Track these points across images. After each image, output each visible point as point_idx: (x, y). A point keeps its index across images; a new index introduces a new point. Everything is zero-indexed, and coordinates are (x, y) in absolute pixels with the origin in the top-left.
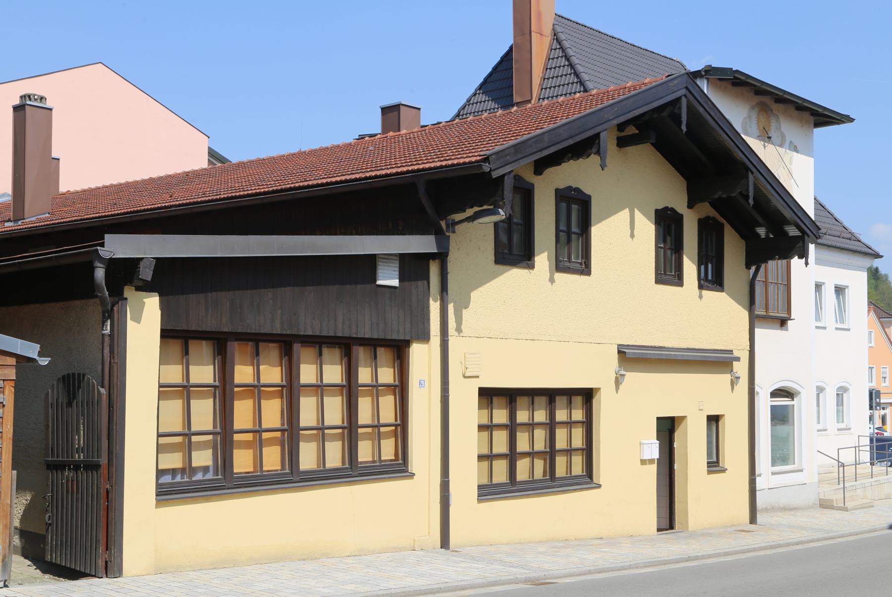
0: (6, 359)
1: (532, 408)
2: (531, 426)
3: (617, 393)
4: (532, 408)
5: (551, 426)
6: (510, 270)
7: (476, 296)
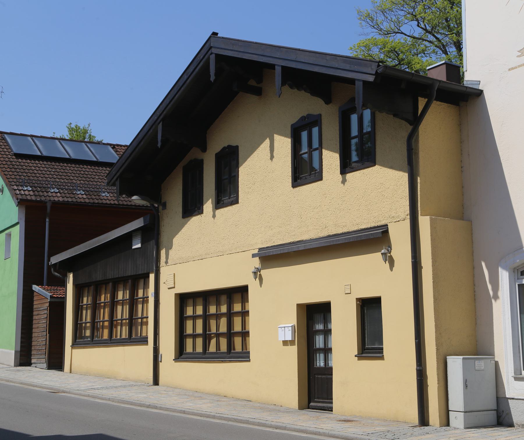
0: (24, 213)
1: (218, 305)
2: (218, 316)
3: (261, 287)
4: (218, 305)
5: (206, 317)
6: (191, 219)
7: (176, 240)
